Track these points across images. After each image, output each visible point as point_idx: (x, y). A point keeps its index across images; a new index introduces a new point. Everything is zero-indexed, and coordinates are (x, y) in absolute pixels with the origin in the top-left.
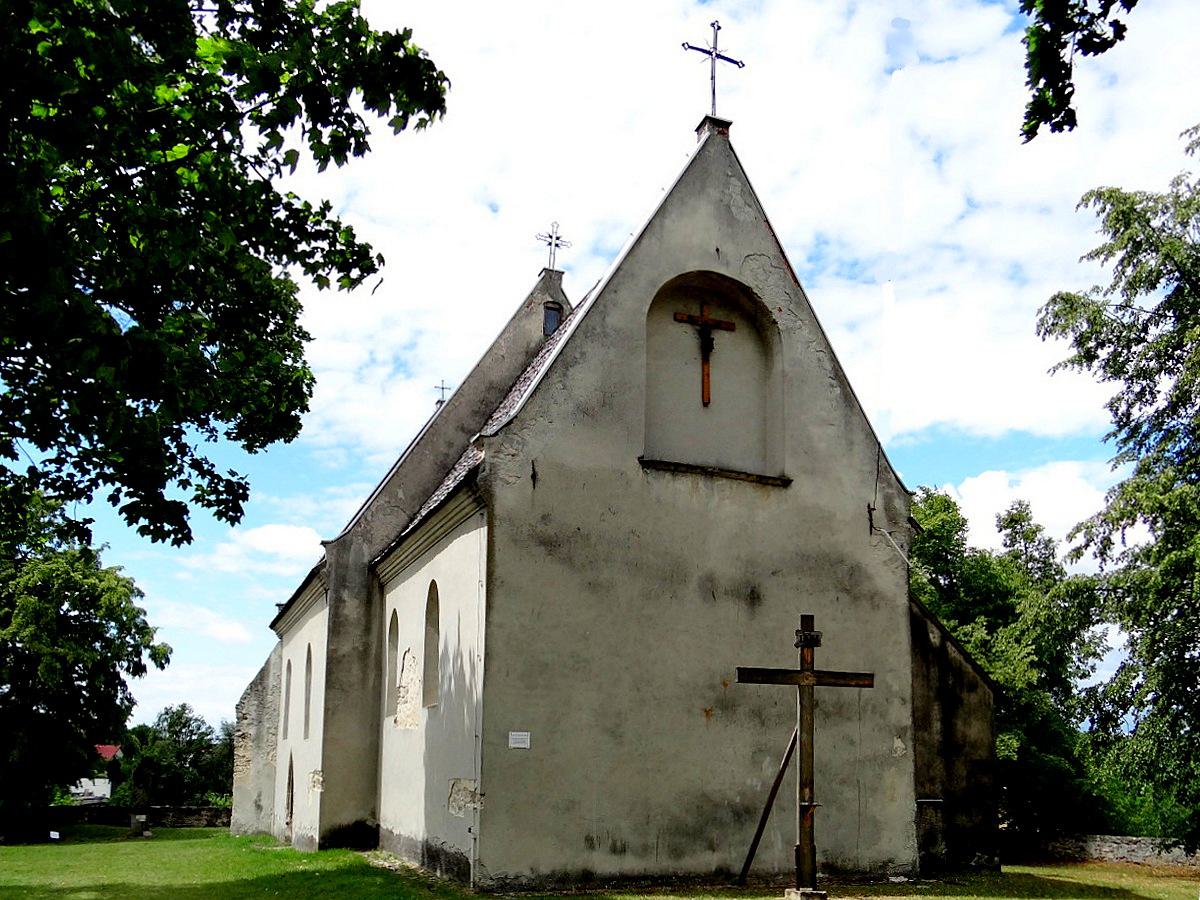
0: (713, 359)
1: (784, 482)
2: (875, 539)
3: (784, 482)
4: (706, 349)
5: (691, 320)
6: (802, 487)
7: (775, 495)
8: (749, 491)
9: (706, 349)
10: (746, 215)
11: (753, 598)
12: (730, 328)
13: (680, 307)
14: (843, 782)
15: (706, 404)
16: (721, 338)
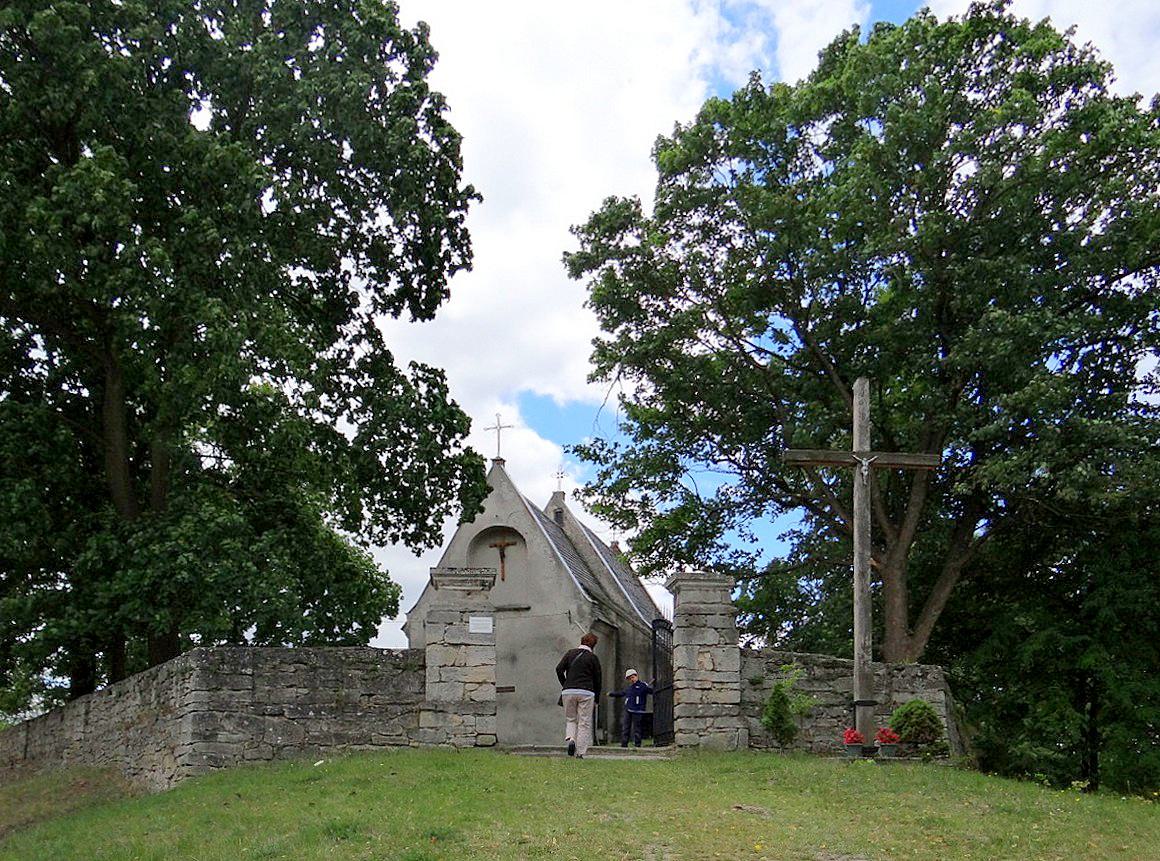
0: (505, 560)
1: (528, 609)
2: (572, 626)
3: (528, 609)
4: (503, 556)
5: (496, 546)
6: (537, 609)
7: (523, 614)
8: (512, 614)
9: (503, 556)
10: (509, 496)
11: (513, 659)
12: (514, 544)
13: (493, 542)
14: (555, 732)
15: (503, 580)
16: (509, 551)
